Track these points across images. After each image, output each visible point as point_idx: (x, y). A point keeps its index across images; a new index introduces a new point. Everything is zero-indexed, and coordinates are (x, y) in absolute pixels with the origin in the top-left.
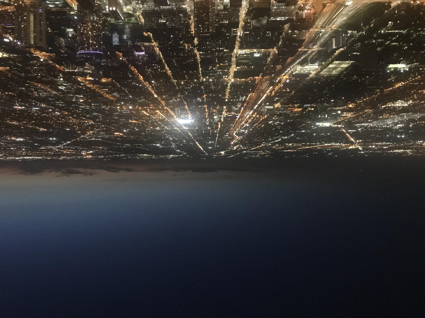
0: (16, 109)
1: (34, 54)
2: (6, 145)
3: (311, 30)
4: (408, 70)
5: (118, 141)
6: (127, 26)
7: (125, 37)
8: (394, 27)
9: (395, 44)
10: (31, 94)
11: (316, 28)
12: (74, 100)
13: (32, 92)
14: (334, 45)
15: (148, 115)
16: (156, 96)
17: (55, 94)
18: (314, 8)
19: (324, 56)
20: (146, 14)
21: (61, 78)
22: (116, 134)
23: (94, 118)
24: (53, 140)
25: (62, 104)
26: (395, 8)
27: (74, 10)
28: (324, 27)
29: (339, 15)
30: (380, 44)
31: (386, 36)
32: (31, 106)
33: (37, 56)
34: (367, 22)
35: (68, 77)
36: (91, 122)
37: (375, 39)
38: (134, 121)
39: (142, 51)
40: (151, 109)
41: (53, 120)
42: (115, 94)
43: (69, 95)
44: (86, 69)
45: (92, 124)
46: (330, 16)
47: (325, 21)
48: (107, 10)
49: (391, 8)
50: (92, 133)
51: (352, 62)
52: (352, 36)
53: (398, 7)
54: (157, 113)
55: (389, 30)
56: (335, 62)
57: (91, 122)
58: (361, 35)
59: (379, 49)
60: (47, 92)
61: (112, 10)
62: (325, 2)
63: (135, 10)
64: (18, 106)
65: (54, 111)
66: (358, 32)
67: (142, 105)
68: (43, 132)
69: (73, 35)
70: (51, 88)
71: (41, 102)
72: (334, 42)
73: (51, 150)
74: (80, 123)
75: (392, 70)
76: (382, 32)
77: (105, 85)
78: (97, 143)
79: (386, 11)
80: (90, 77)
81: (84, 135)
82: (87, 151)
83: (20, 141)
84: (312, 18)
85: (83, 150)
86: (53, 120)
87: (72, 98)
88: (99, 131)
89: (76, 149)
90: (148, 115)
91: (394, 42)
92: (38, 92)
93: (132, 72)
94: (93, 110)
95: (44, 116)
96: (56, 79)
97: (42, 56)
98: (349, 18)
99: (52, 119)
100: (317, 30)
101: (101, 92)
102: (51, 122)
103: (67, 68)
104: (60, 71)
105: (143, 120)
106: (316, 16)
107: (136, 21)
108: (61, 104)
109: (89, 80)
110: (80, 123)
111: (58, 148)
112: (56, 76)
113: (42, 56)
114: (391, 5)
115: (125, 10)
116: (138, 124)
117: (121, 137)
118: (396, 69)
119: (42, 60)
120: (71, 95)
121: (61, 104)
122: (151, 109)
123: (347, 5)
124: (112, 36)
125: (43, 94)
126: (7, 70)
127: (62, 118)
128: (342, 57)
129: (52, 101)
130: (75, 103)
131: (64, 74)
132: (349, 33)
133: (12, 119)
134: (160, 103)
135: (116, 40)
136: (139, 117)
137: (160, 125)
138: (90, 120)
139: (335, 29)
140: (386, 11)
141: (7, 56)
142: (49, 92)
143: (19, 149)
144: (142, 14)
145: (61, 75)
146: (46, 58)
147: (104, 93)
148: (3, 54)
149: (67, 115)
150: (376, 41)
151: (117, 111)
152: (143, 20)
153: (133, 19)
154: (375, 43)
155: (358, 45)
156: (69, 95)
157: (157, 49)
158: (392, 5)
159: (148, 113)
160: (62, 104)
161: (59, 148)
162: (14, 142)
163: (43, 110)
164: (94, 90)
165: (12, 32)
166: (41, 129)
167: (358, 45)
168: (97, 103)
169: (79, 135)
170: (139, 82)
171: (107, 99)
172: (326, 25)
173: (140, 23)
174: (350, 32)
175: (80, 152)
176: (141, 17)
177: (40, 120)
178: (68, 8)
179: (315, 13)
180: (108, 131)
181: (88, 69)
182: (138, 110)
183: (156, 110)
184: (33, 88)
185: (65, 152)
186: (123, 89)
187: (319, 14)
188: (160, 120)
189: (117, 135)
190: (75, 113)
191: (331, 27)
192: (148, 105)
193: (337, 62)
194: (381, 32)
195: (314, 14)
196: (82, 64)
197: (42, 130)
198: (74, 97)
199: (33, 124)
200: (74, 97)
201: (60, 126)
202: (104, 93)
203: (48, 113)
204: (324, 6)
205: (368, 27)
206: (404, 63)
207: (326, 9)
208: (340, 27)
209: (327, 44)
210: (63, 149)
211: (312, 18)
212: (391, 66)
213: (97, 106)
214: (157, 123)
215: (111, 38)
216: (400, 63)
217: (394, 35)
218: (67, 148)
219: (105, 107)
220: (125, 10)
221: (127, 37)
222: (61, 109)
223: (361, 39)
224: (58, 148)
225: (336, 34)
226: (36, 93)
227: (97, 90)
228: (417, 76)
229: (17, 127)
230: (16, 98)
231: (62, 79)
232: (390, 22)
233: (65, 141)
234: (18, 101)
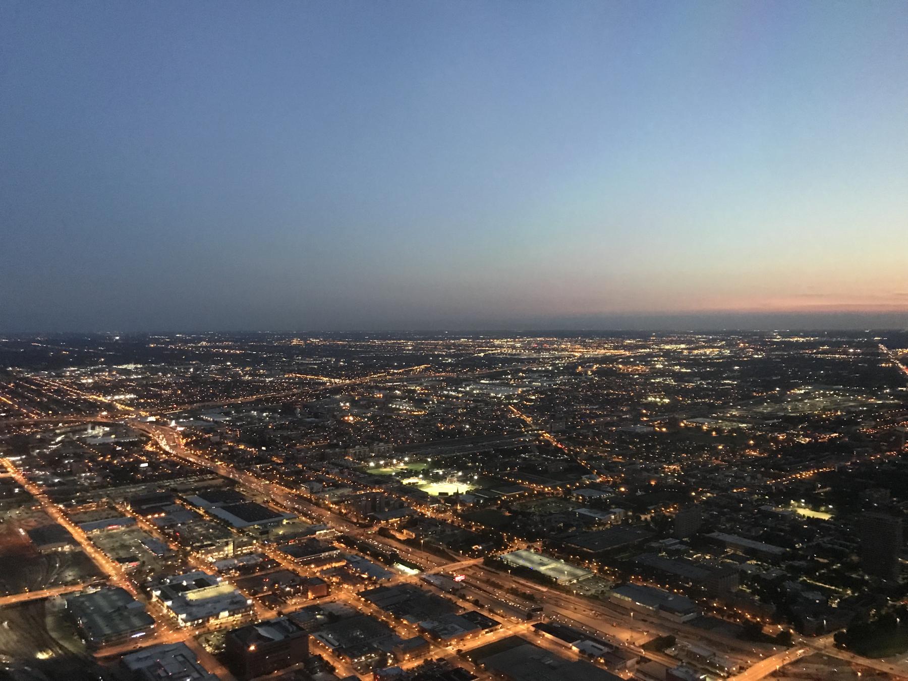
4: (792, 502)
8: (828, 594)
9: (821, 560)
26: (829, 632)
30: (854, 567)
34: (885, 622)
37: (866, 583)
49: (835, 635)
53: (820, 632)
55: (834, 591)
58: (898, 600)
59: (855, 558)
75: (823, 509)
76: (849, 592)
91: (823, 563)
114: (835, 640)
118: (816, 509)
150: (863, 577)
167: (904, 579)
194: (853, 593)
205: (883, 612)
206: (799, 516)
212: (826, 517)
216: (808, 517)
228: (774, 484)
232: (834, 606)
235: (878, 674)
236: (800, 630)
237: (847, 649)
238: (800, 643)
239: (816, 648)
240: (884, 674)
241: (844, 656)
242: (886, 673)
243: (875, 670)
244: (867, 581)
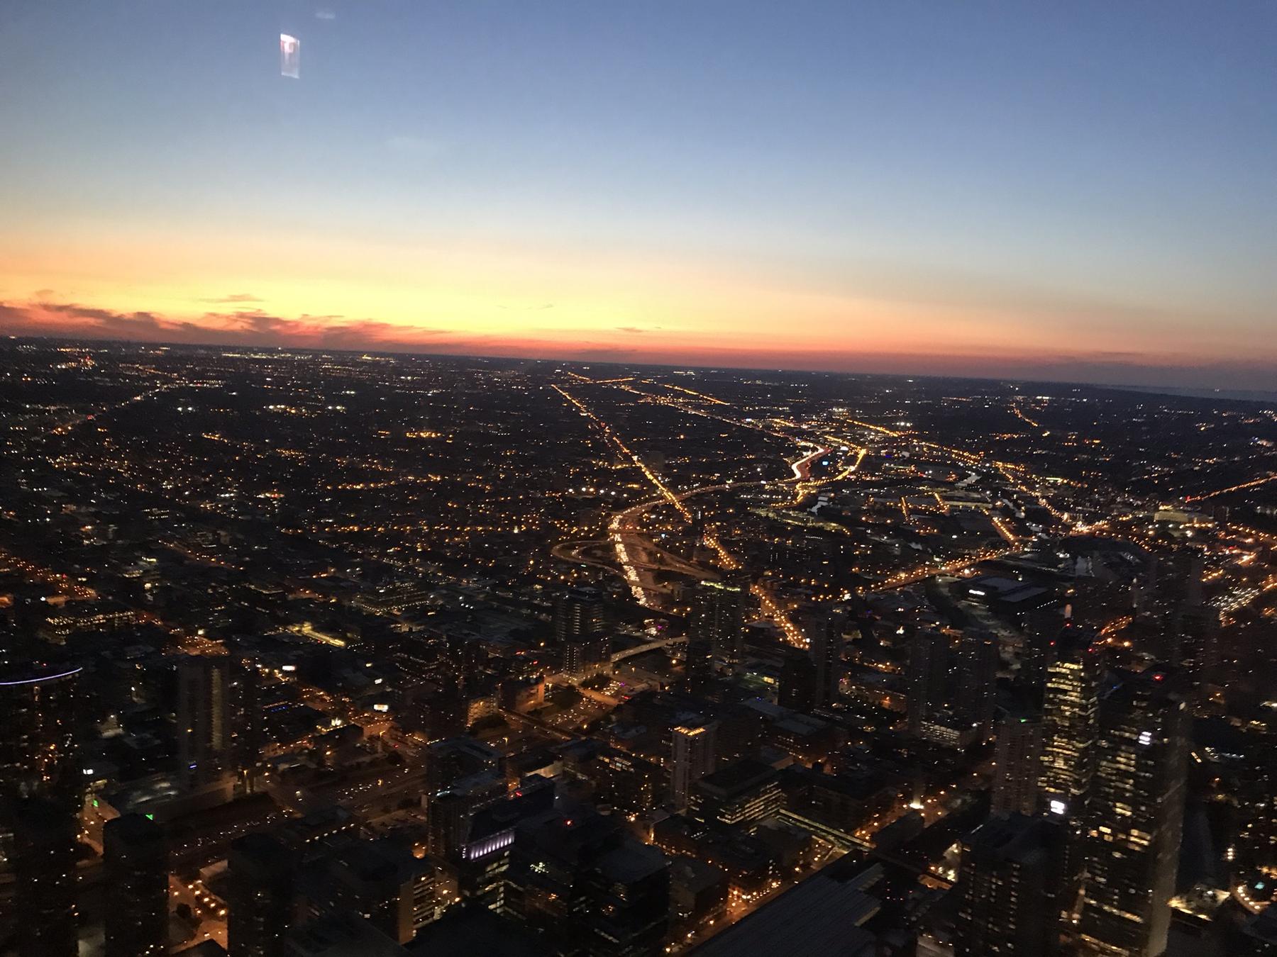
0: (279, 492)
1: (222, 644)
10: (240, 536)
13: (234, 542)
21: (150, 590)
24: (185, 406)
25: (151, 514)
32: (240, 502)
33: (212, 639)
41: (180, 464)
64: (275, 499)
65: (177, 491)
69: (105, 720)
73: (193, 376)
74: (97, 460)
78: (41, 395)
86: (180, 464)
87: (118, 534)
89: (113, 376)
92: (217, 541)
97: (202, 643)
99: (186, 468)
102: (187, 460)
104: (151, 608)
108: (156, 514)
111: (172, 381)
113: (202, 643)
119: (201, 632)
120: (120, 542)
121: (156, 514)
125: (205, 537)
127: (153, 472)
129: (179, 521)
133: (294, 460)
145: (150, 598)
146: (188, 640)
148: (299, 631)
149: (136, 480)
160: (151, 514)
161: (166, 380)
169: (101, 421)
175: (101, 367)
178: (113, 793)
181: (58, 627)
190: (109, 489)
197: (214, 434)
198: (111, 536)
200: (111, 536)
201: (163, 447)
202: (6, 559)
210: (156, 377)
218: (144, 380)
222: (157, 499)
224: (172, 381)
226: (222, 540)
231: (148, 586)
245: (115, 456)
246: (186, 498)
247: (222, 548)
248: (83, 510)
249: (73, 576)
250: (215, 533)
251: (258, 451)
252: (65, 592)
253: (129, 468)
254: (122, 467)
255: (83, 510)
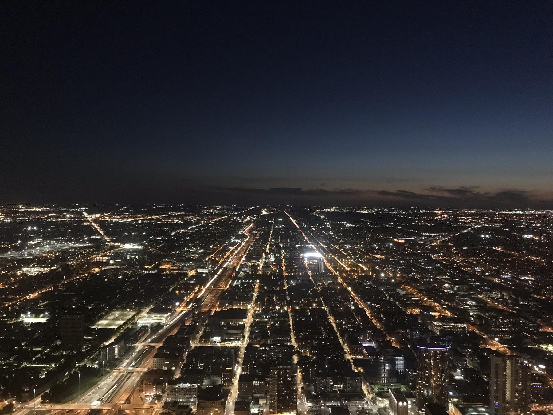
0: (532, 277)
1: (507, 347)
2: (546, 229)
3: (145, 370)
4: (22, 315)
5: (399, 231)
6: (385, 380)
7: (387, 367)
8: (38, 371)
9: (37, 349)
11: (138, 372)
12: (456, 286)
13: (510, 298)
14: (116, 350)
15: (360, 265)
16: (350, 289)
17: (481, 294)
18: (141, 398)
19: (129, 335)
20: (360, 396)
21: (472, 316)
22: (403, 241)
23: (431, 262)
24: (485, 234)
26: (37, 395)
27: (454, 403)
28: (129, 372)
29: (109, 387)
30: (57, 348)
31: (49, 359)
32: (512, 280)
35: (462, 316)
36: (435, 257)
37: (63, 356)
38: (379, 256)
39: (365, 348)
40: (357, 272)
41: (484, 261)
42: (402, 293)
43: (462, 293)
44: (439, 326)
45: (433, 255)
46: (122, 387)
47: (127, 381)
48: (409, 402)
49: (42, 396)
50: (433, 243)
51: (94, 327)
52: (93, 361)
53: (32, 397)
54: (348, 267)
56: (116, 327)
57: (435, 257)
59: (59, 343)
60: (491, 298)
61: (403, 402)
62: (127, 405)
63: (374, 401)
64: (530, 280)
65: (483, 273)
66: (85, 365)
67: (367, 278)
68: (497, 246)
69: (455, 371)
70: (485, 303)
71: (499, 284)
72: (116, 354)
73: (488, 222)
75: (42, 315)
76: (53, 365)
77: (416, 305)
79: (48, 391)
80: (435, 316)
81: (445, 241)
82: (441, 219)
83: (528, 234)
84: (144, 385)
85: (446, 221)
86: (484, 261)
87: (458, 289)
88: (424, 245)
89: (455, 222)
90: (360, 265)
92: (502, 297)
93: (380, 320)
94: (432, 273)
95: (495, 266)
96: (479, 314)
98: (96, 383)
99: (486, 262)
100: (138, 369)
101: (421, 296)
103: (464, 329)
104: (473, 324)
105: (367, 258)
106: (138, 388)
107: (373, 386)
108: (474, 282)
109: (435, 311)
110: (449, 256)
112: (478, 317)
113: (496, 345)
115: (387, 402)
116: (373, 253)
117: (396, 236)
118: (37, 316)
119: (497, 339)
120: (459, 292)
121: (474, 282)
122: (357, 272)
123: (98, 400)
124: (405, 368)
126: (542, 327)
127: (472, 263)
128: (106, 333)
129: (484, 286)
130: (454, 283)
131: (468, 321)
132: (97, 364)
134: (345, 279)
135: (400, 363)
136: (372, 262)
137: (346, 250)
138: (435, 260)
139: (114, 371)
140: (48, 391)
141: (542, 346)
142: (489, 298)
143: (530, 224)
144: (365, 395)
147: (417, 294)
148: (546, 348)
149: (465, 266)
150: (62, 353)
151: (400, 270)
152: (364, 388)
153: (376, 390)
154: (64, 350)
155: (86, 348)
156: (462, 293)
157: (346, 349)
158: (40, 399)
159: (359, 267)
161: (477, 223)
162: (535, 234)
163: (497, 274)
164: (430, 298)
165: (534, 377)
166: (500, 249)
167: (86, 348)
168: (426, 281)
170: (371, 308)
171: (412, 287)
172: (126, 376)
173: (368, 384)
174: (96, 366)
176: (366, 392)
177: (501, 261)
178: (461, 406)
179: (140, 391)
180: (412, 244)
181: (436, 325)
182: (374, 271)
183: (349, 271)
184: (509, 304)
185: (469, 219)
186: (391, 299)
187: (134, 390)
188: (345, 257)
189: (402, 240)
191: (120, 372)
192: (360, 277)
193: (112, 327)
194: (55, 365)
195: (141, 391)
196: (445, 333)
199: (510, 256)
201: (475, 252)
203: (490, 270)
204: (128, 401)
205: (72, 372)
206: (27, 324)
207: (125, 397)
208: (109, 372)
209: (126, 351)
210: (472, 222)
211: (144, 385)
212: (43, 320)
213: (426, 278)
214: (349, 254)
215: (405, 366)
217: (38, 361)
218: (467, 223)
219: (416, 277)
220: (387, 402)
221: (385, 366)
222: (474, 275)
223: (81, 356)
225: (114, 364)
226: (505, 297)
227: (426, 299)
228: (10, 306)
229: (532, 253)
230: (532, 290)
231: (471, 314)
232: (43, 377)
233: (469, 232)
234: (529, 286)
235: (67, 412)
236: (20, 400)
237: (50, 402)
238: (19, 408)
239: (28, 408)
240: (71, 411)
241: (48, 407)
242: (72, 410)
243: (66, 410)
244: (64, 355)
245: (457, 254)
246: (487, 276)
247: (505, 301)
248: (444, 277)
249: (442, 305)
250: (501, 294)
251: (520, 257)
252: (439, 311)
253: (462, 261)
254: (459, 260)
255: (444, 277)
